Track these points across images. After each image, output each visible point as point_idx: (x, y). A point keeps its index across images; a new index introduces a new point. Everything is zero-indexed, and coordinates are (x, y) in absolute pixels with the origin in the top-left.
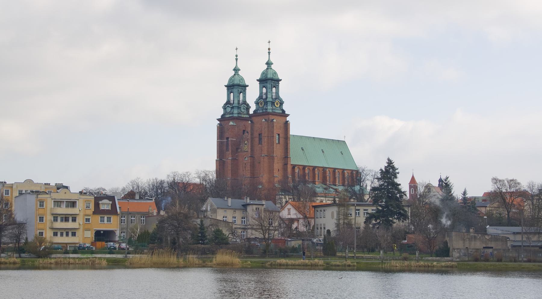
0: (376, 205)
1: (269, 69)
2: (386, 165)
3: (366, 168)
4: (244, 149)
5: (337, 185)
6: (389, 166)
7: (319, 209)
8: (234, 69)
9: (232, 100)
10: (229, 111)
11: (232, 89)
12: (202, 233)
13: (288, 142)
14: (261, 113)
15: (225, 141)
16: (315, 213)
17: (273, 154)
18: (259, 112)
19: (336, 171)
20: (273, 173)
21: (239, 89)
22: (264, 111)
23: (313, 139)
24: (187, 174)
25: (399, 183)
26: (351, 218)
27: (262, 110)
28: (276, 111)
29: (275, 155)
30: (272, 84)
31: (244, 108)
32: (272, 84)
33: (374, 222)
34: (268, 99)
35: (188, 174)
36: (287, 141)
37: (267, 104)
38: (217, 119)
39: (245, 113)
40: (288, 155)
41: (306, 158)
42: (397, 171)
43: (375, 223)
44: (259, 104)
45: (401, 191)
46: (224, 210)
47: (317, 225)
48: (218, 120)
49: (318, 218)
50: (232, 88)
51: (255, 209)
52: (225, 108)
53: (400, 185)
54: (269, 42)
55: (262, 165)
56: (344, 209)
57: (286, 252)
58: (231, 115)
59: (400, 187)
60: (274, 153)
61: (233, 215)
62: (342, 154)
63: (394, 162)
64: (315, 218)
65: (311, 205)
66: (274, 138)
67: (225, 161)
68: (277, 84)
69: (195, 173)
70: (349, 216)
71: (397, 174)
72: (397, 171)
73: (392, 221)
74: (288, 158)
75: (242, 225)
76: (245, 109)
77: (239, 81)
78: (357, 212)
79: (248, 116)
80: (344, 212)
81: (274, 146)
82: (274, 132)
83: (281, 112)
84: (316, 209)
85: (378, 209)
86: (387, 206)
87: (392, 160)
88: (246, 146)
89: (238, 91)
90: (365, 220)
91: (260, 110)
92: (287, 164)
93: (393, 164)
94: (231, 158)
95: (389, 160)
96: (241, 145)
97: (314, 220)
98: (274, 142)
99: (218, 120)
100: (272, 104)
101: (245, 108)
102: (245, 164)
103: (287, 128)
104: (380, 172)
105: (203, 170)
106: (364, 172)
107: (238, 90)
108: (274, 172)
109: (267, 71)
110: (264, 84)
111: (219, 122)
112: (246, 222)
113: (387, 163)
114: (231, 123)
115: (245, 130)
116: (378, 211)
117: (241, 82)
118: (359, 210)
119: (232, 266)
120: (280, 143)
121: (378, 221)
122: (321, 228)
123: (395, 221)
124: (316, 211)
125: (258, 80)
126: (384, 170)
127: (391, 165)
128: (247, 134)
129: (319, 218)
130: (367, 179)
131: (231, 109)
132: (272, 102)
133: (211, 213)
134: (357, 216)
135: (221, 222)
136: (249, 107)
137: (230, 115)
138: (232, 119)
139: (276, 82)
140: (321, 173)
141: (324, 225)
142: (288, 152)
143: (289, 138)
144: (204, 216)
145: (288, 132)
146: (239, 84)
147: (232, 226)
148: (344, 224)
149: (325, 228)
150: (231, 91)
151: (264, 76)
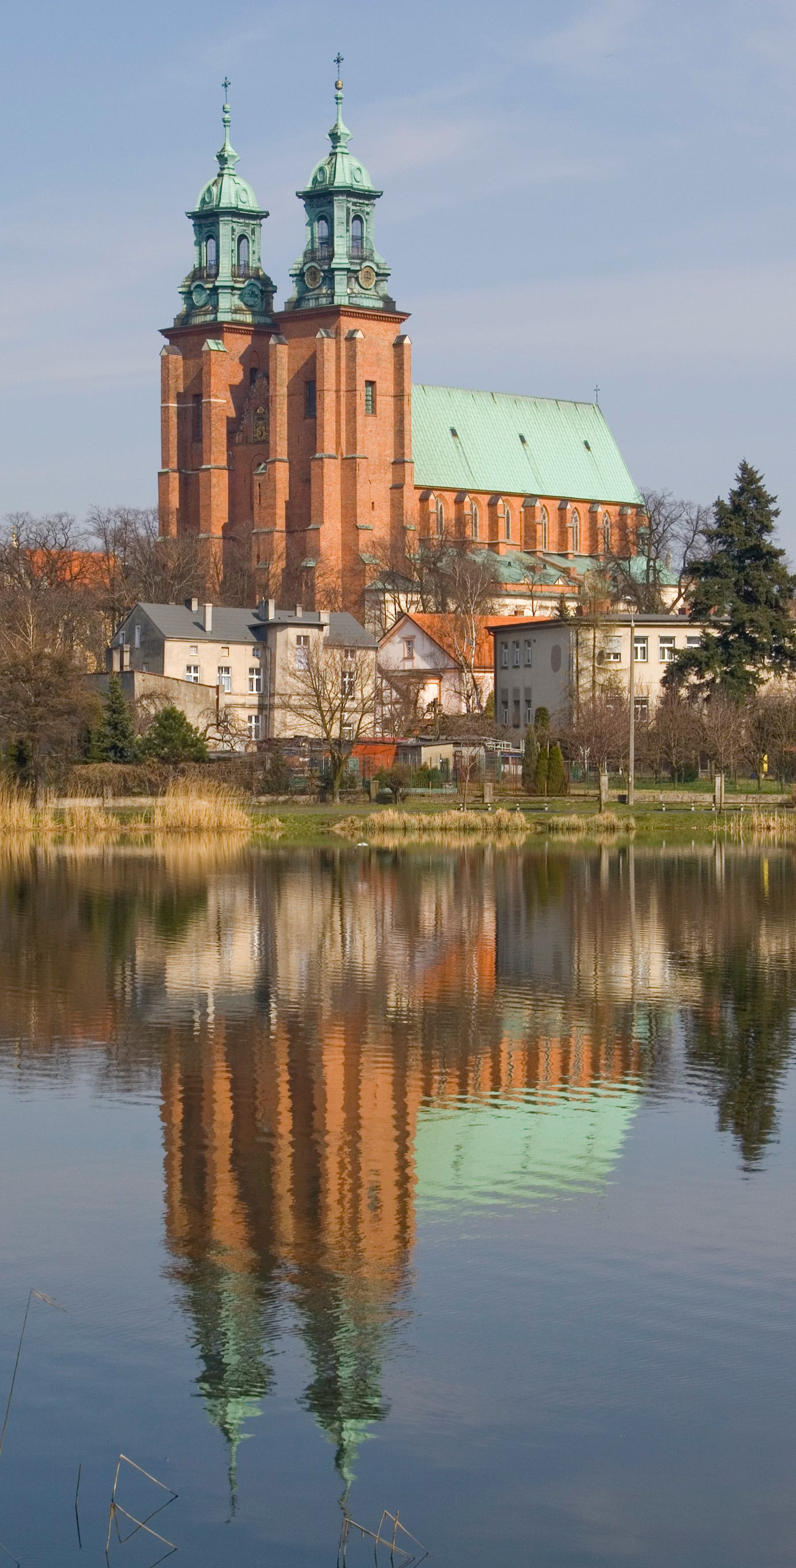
0: (700, 621)
1: (339, 155)
2: (736, 486)
3: (669, 495)
4: (254, 433)
5: (571, 557)
6: (742, 490)
7: (510, 639)
9: (213, 263)
11: (212, 224)
12: (116, 724)
13: (406, 408)
14: (312, 309)
16: (498, 653)
17: (355, 452)
19: (569, 507)
20: (355, 516)
21: (235, 225)
22: (324, 301)
23: (491, 398)
24: (62, 523)
25: (777, 546)
26: (619, 666)
28: (364, 300)
29: (362, 455)
30: (348, 209)
31: (253, 293)
32: (348, 209)
33: (693, 679)
34: (334, 261)
35: (64, 520)
36: (403, 405)
37: (332, 279)
38: (161, 331)
39: (256, 309)
40: (403, 454)
41: (465, 464)
42: (772, 507)
43: (697, 682)
45: (785, 575)
46: (188, 644)
47: (505, 692)
48: (165, 333)
49: (506, 668)
50: (211, 220)
51: (293, 639)
52: (188, 295)
53: (781, 552)
54: (338, 61)
55: (317, 490)
56: (595, 637)
57: (400, 784)
59: (781, 559)
60: (358, 447)
61: (219, 661)
62: (588, 447)
63: (761, 478)
64: (498, 667)
65: (483, 625)
66: (356, 395)
68: (367, 209)
69: (89, 517)
70: (612, 659)
71: (773, 518)
72: (772, 507)
73: (752, 675)
74: (406, 465)
75: (250, 695)
76: (256, 296)
77: (237, 195)
78: (639, 646)
79: (268, 320)
80: (594, 646)
81: (355, 422)
82: (358, 375)
83: (380, 304)
84: (501, 638)
85: (707, 635)
86: (738, 628)
87: (755, 469)
88: (261, 422)
89: (233, 234)
90: (665, 672)
92: (402, 487)
93: (760, 484)
95: (744, 468)
96: (245, 422)
97: (493, 675)
98: (355, 409)
99: (165, 333)
100: (349, 279)
101: (257, 292)
103: (403, 360)
104: (715, 509)
105: (115, 509)
106: (663, 511)
107: (233, 230)
108: (359, 511)
109: (334, 161)
111: (167, 342)
112: (265, 687)
113: (739, 480)
115: (256, 367)
116: (707, 644)
117: (244, 200)
118: (644, 639)
119: (219, 833)
120: (378, 412)
121: (708, 676)
122: (517, 703)
123: (763, 675)
124: (499, 645)
125: (300, 195)
126: (727, 502)
127: (754, 486)
128: (265, 382)
129: (510, 668)
130: (673, 536)
132: (348, 270)
133: (147, 656)
134: (639, 659)
135: (179, 685)
136: (270, 289)
137: (205, 315)
139: (361, 201)
140: (517, 513)
141: (528, 691)
142: (406, 442)
143: (409, 395)
144: (122, 667)
145: (406, 374)
146: (236, 208)
147: (218, 700)
148: (594, 689)
149: (528, 702)
150: (209, 231)
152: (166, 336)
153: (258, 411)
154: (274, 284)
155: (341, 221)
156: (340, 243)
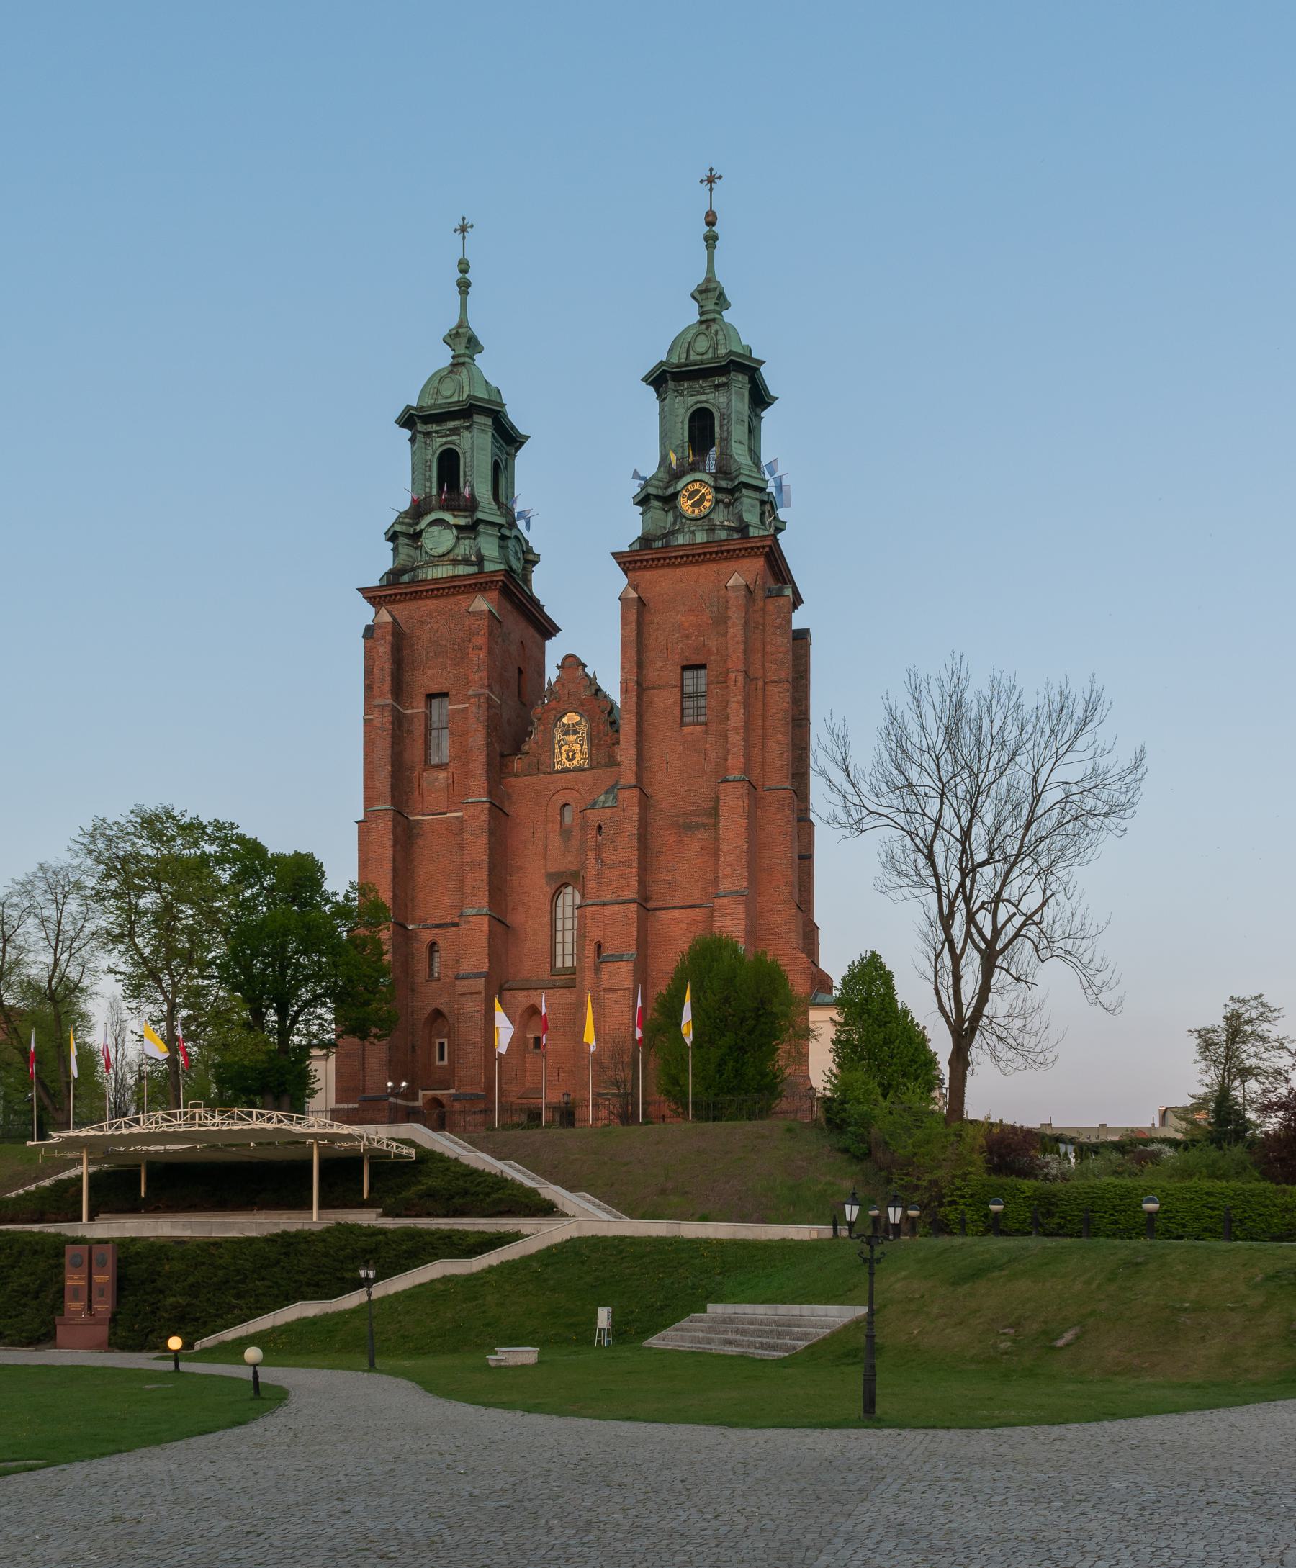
8: (450, 335)
10: (441, 550)
11: (455, 431)
18: (680, 540)
22: (723, 535)
27: (711, 530)
50: (451, 424)
58: (462, 570)
67: (417, 821)
88: (571, 738)
91: (693, 532)
110: (703, 398)
114: (481, 604)
131: (458, 538)
150: (446, 443)
151: (702, 350)
153: (565, 720)
156: (740, 452)
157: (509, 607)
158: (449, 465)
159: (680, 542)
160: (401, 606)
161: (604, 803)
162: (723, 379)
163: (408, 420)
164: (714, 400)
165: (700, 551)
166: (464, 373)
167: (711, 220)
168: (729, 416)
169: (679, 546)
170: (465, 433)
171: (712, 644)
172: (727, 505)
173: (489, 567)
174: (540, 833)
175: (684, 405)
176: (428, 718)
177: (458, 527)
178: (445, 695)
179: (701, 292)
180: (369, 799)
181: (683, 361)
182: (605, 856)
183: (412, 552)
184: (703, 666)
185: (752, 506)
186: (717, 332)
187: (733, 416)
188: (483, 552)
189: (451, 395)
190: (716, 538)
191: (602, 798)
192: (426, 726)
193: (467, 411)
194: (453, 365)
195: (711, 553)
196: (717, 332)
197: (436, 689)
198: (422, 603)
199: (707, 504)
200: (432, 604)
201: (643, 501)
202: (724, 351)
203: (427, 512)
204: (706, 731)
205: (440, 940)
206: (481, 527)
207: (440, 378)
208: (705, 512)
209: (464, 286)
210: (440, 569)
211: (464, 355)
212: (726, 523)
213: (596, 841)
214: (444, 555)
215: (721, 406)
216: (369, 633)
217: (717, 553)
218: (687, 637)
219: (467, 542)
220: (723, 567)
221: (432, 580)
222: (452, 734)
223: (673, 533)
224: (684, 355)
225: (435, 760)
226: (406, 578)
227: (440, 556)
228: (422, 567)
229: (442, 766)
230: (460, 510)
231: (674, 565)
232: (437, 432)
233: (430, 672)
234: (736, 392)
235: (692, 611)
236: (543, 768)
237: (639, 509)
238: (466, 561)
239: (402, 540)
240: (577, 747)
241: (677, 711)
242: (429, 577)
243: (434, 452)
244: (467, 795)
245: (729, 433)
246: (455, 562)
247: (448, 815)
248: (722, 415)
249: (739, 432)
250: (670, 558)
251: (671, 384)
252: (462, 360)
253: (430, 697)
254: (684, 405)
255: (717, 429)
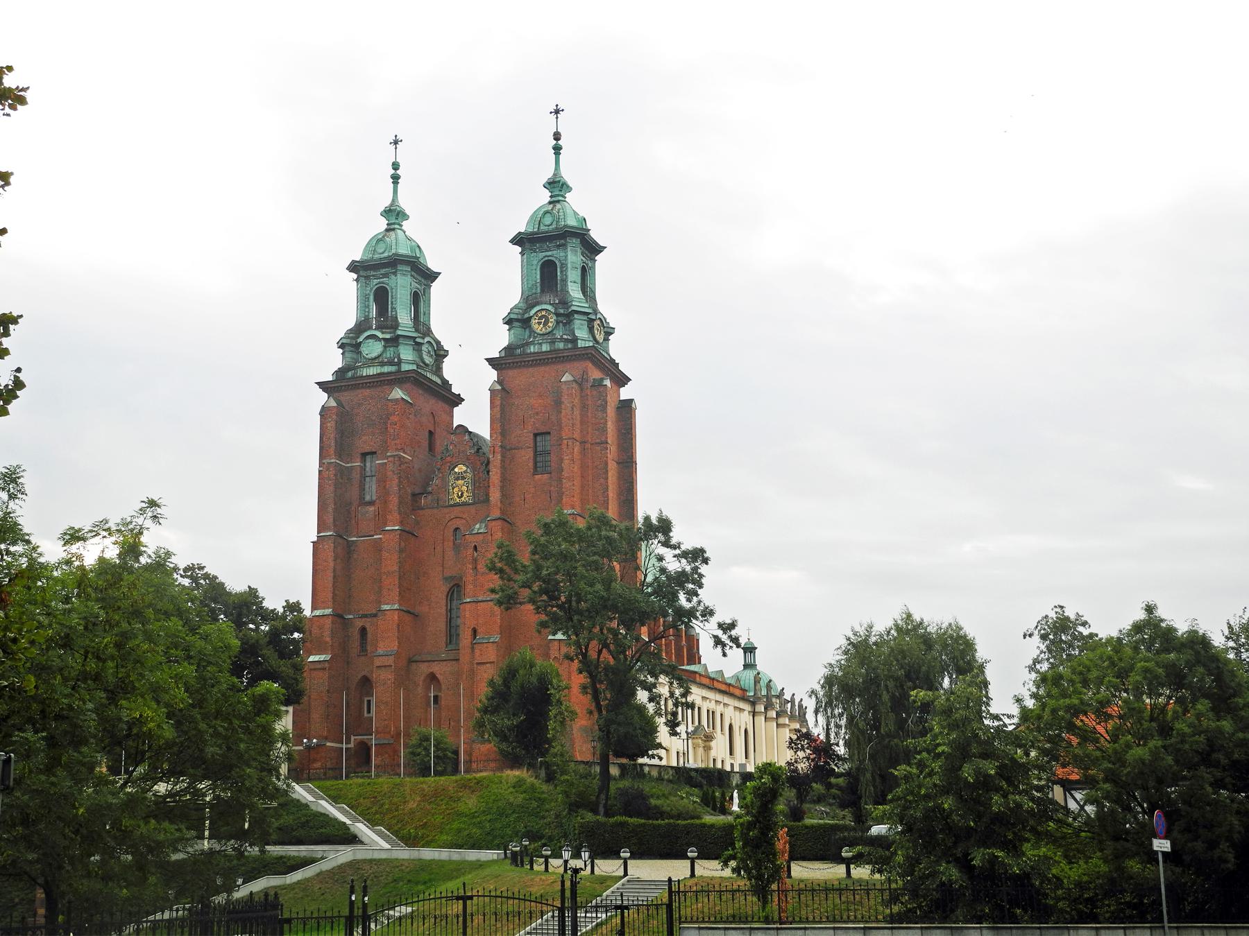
8: (385, 211)
10: (374, 355)
11: (386, 275)
15: (359, 464)
18: (532, 349)
22: (561, 345)
27: (553, 342)
44: (534, 322)
48: (323, 386)
50: (383, 271)
58: (386, 369)
88: (460, 482)
91: (541, 344)
94: (397, 528)
99: (323, 386)
102: (475, 547)
110: (550, 253)
114: (398, 393)
131: (385, 347)
136: (442, 353)
138: (400, 379)
152: (325, 390)
153: (456, 470)
154: (445, 348)
155: (574, 265)
157: (421, 392)
158: (382, 297)
159: (532, 350)
160: (346, 394)
161: (478, 529)
162: (563, 241)
163: (354, 267)
164: (555, 254)
165: (544, 357)
166: (392, 233)
167: (557, 136)
168: (566, 265)
169: (531, 353)
170: (393, 277)
171: (553, 418)
172: (565, 324)
173: (405, 367)
174: (439, 549)
175: (538, 258)
176: (363, 469)
177: (383, 339)
178: (375, 453)
179: (550, 183)
180: (321, 526)
181: (536, 230)
182: (479, 567)
183: (355, 356)
184: (549, 433)
185: (582, 325)
186: (559, 210)
187: (569, 265)
188: (402, 357)
189: (383, 253)
190: (556, 347)
191: (478, 526)
192: (361, 474)
193: (393, 263)
194: (387, 230)
195: (552, 358)
196: (559, 210)
197: (367, 449)
198: (360, 391)
199: (550, 324)
200: (367, 392)
201: (509, 321)
202: (563, 223)
203: (365, 331)
204: (551, 477)
205: (367, 626)
206: (401, 340)
207: (379, 240)
208: (550, 330)
209: (396, 179)
210: (372, 368)
211: (394, 224)
212: (565, 337)
213: (473, 556)
214: (376, 358)
215: (562, 259)
216: (324, 412)
217: (556, 358)
218: (537, 413)
219: (392, 349)
220: (560, 367)
221: (367, 376)
222: (378, 481)
223: (528, 344)
224: (537, 226)
225: (368, 498)
226: (350, 374)
227: (372, 359)
228: (360, 367)
229: (371, 503)
230: (387, 328)
231: (528, 366)
232: (373, 276)
233: (364, 438)
234: (571, 250)
235: (540, 396)
236: (441, 503)
237: (507, 327)
238: (391, 363)
239: (347, 348)
240: (465, 488)
241: (531, 464)
242: (364, 374)
243: (371, 289)
244: (386, 525)
245: (567, 276)
246: (382, 364)
247: (375, 537)
248: (562, 264)
249: (573, 276)
250: (525, 362)
251: (527, 245)
252: (392, 227)
253: (364, 455)
254: (538, 258)
255: (559, 274)
